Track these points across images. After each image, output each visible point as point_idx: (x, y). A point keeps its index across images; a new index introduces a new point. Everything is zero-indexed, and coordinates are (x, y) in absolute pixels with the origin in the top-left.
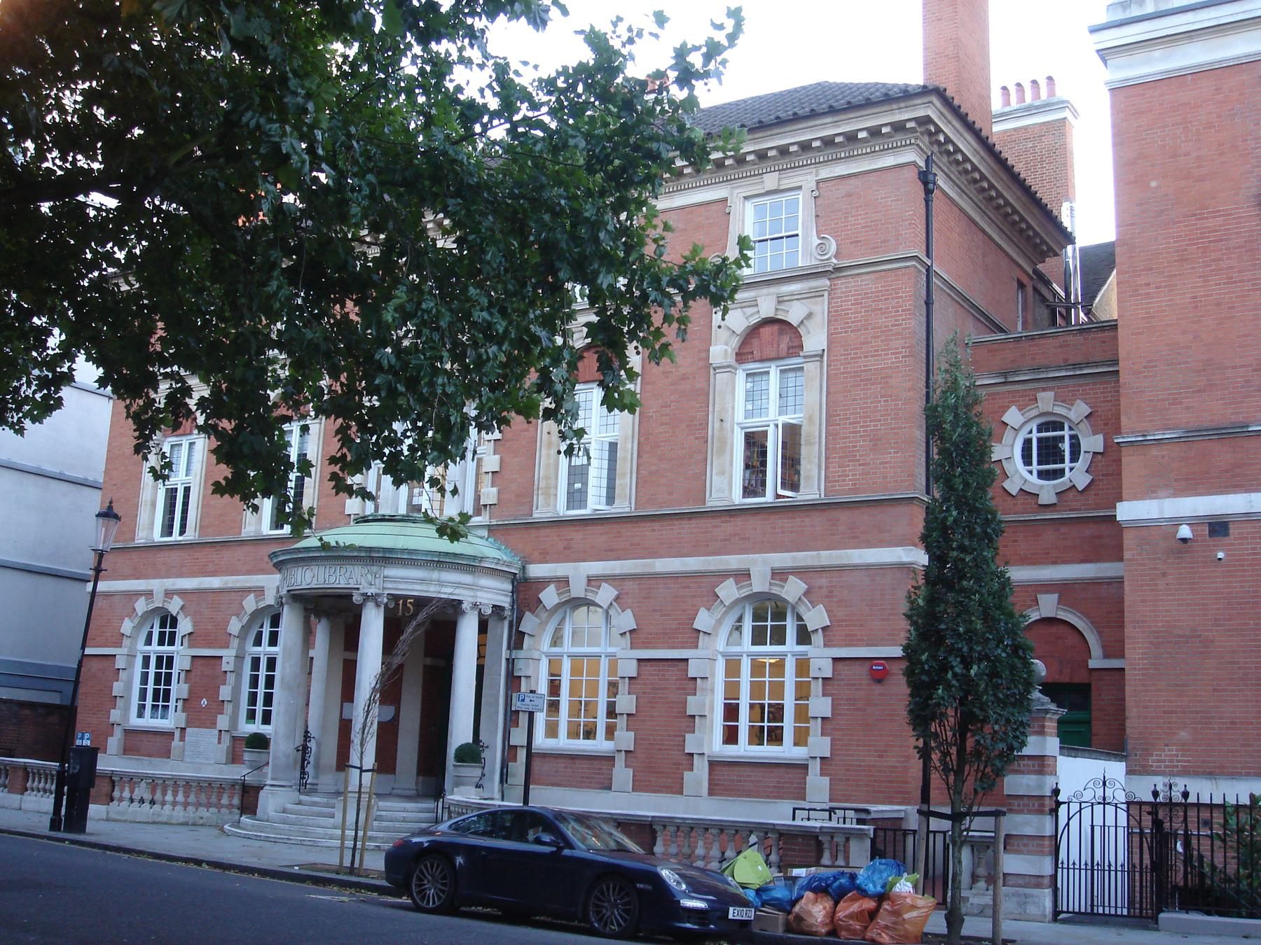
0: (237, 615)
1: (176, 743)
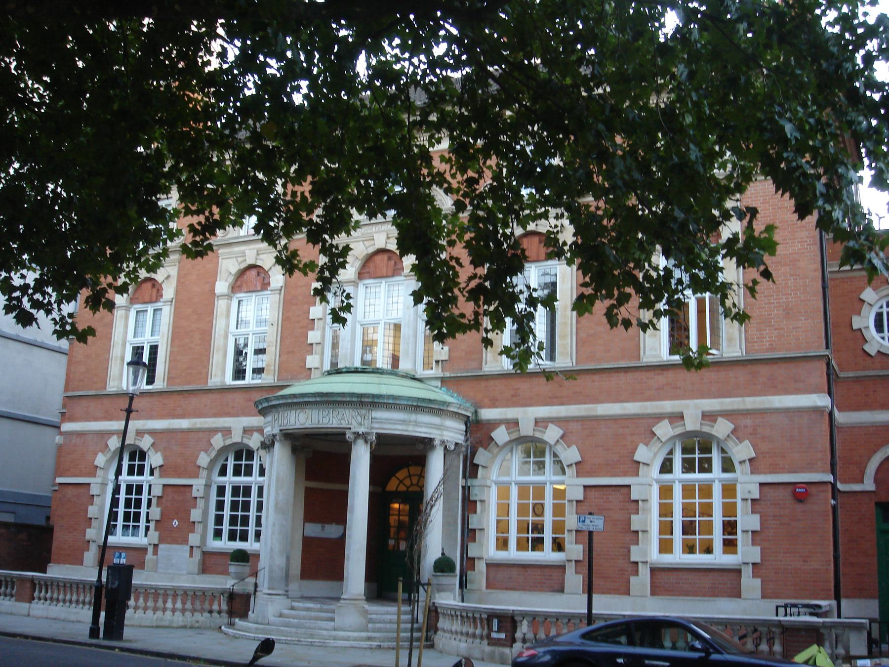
0: (206, 451)
1: (149, 556)
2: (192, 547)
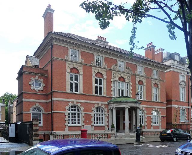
2: (92, 126)
